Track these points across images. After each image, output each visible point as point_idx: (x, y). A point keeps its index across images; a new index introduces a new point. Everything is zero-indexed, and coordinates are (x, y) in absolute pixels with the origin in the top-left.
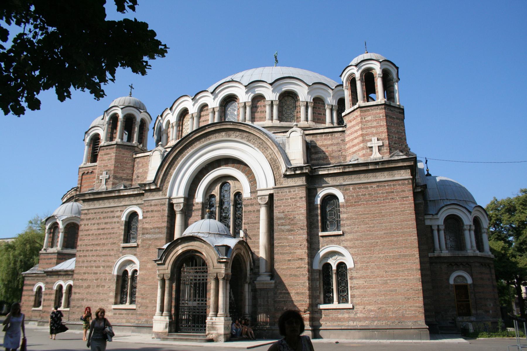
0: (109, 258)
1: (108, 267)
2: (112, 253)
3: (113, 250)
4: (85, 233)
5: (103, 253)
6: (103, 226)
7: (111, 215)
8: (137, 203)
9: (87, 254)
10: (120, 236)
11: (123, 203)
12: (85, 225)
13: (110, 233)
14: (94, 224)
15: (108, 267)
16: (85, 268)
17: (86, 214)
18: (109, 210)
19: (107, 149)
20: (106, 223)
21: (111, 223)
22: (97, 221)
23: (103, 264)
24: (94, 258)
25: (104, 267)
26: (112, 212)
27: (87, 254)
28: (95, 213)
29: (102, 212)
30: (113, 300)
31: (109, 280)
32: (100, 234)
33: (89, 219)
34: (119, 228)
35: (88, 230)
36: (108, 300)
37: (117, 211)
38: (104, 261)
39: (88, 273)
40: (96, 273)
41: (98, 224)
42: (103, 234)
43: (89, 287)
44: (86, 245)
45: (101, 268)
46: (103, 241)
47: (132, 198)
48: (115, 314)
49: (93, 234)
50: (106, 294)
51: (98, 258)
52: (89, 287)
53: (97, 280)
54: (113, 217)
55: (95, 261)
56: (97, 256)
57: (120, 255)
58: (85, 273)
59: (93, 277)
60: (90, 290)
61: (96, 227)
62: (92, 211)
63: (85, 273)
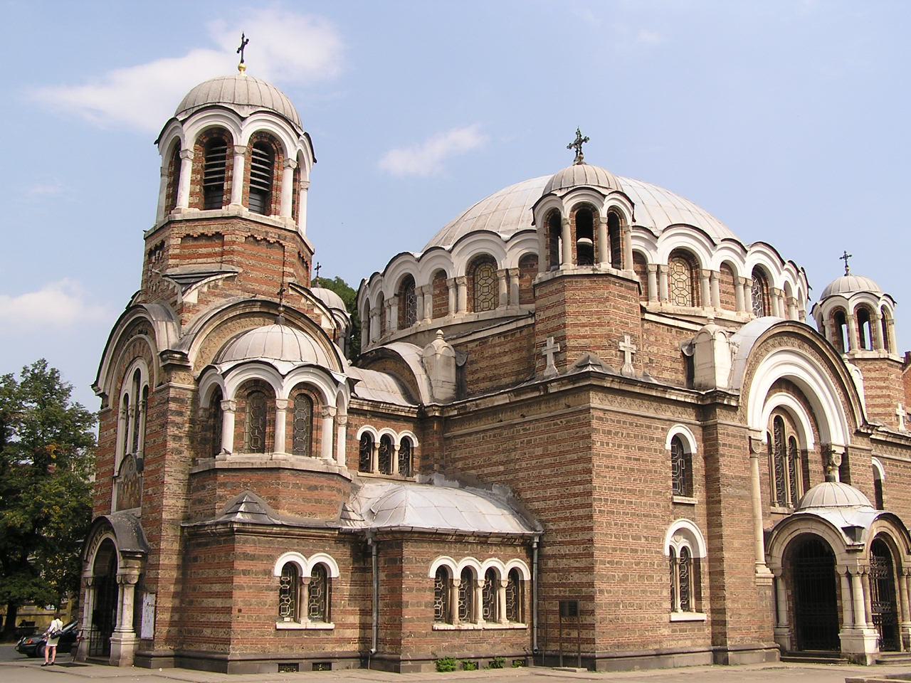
0: (654, 522)
1: (655, 538)
2: (658, 512)
3: (658, 505)
4: (605, 462)
5: (642, 511)
6: (637, 454)
7: (648, 433)
8: (687, 421)
9: (614, 508)
10: (666, 479)
11: (668, 415)
12: (602, 444)
13: (650, 471)
14: (619, 446)
15: (655, 538)
16: (613, 539)
17: (600, 419)
18: (642, 421)
19: (621, 285)
20: (640, 449)
21: (649, 450)
22: (624, 442)
23: (645, 533)
24: (627, 519)
25: (646, 538)
26: (649, 427)
27: (614, 508)
28: (619, 422)
29: (631, 424)
30: (667, 605)
31: (659, 565)
32: (632, 470)
33: (609, 432)
34: (663, 462)
35: (609, 457)
36: (661, 604)
37: (657, 428)
38: (646, 527)
39: (621, 549)
40: (636, 551)
41: (627, 447)
42: (638, 470)
43: (625, 578)
44: (610, 489)
45: (643, 540)
46: (641, 486)
47: (680, 409)
48: (674, 631)
49: (619, 468)
50: (656, 592)
51: (636, 521)
52: (625, 578)
53: (637, 564)
54: (652, 439)
55: (630, 525)
56: (633, 514)
57: (672, 517)
58: (615, 550)
59: (627, 558)
60: (629, 585)
61: (622, 453)
62: (612, 416)
63: (615, 550)
